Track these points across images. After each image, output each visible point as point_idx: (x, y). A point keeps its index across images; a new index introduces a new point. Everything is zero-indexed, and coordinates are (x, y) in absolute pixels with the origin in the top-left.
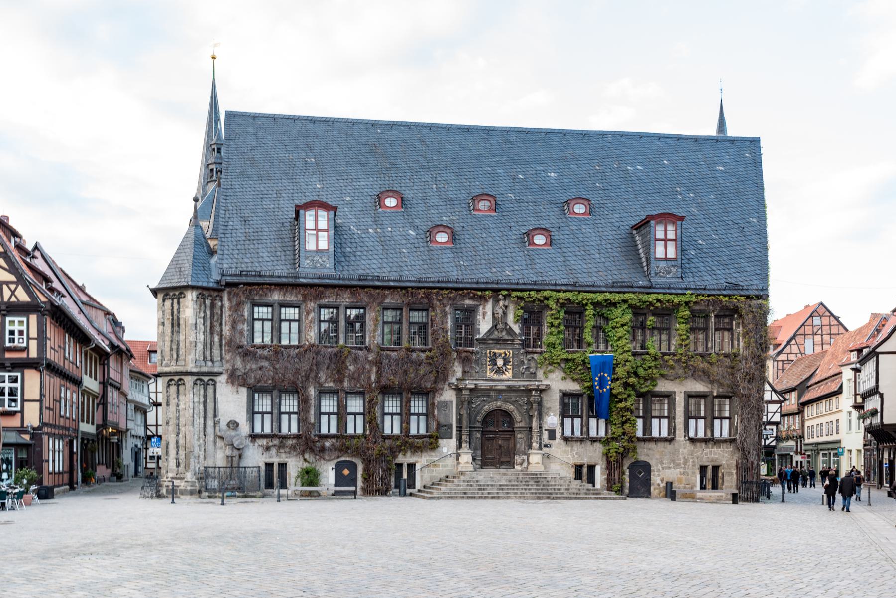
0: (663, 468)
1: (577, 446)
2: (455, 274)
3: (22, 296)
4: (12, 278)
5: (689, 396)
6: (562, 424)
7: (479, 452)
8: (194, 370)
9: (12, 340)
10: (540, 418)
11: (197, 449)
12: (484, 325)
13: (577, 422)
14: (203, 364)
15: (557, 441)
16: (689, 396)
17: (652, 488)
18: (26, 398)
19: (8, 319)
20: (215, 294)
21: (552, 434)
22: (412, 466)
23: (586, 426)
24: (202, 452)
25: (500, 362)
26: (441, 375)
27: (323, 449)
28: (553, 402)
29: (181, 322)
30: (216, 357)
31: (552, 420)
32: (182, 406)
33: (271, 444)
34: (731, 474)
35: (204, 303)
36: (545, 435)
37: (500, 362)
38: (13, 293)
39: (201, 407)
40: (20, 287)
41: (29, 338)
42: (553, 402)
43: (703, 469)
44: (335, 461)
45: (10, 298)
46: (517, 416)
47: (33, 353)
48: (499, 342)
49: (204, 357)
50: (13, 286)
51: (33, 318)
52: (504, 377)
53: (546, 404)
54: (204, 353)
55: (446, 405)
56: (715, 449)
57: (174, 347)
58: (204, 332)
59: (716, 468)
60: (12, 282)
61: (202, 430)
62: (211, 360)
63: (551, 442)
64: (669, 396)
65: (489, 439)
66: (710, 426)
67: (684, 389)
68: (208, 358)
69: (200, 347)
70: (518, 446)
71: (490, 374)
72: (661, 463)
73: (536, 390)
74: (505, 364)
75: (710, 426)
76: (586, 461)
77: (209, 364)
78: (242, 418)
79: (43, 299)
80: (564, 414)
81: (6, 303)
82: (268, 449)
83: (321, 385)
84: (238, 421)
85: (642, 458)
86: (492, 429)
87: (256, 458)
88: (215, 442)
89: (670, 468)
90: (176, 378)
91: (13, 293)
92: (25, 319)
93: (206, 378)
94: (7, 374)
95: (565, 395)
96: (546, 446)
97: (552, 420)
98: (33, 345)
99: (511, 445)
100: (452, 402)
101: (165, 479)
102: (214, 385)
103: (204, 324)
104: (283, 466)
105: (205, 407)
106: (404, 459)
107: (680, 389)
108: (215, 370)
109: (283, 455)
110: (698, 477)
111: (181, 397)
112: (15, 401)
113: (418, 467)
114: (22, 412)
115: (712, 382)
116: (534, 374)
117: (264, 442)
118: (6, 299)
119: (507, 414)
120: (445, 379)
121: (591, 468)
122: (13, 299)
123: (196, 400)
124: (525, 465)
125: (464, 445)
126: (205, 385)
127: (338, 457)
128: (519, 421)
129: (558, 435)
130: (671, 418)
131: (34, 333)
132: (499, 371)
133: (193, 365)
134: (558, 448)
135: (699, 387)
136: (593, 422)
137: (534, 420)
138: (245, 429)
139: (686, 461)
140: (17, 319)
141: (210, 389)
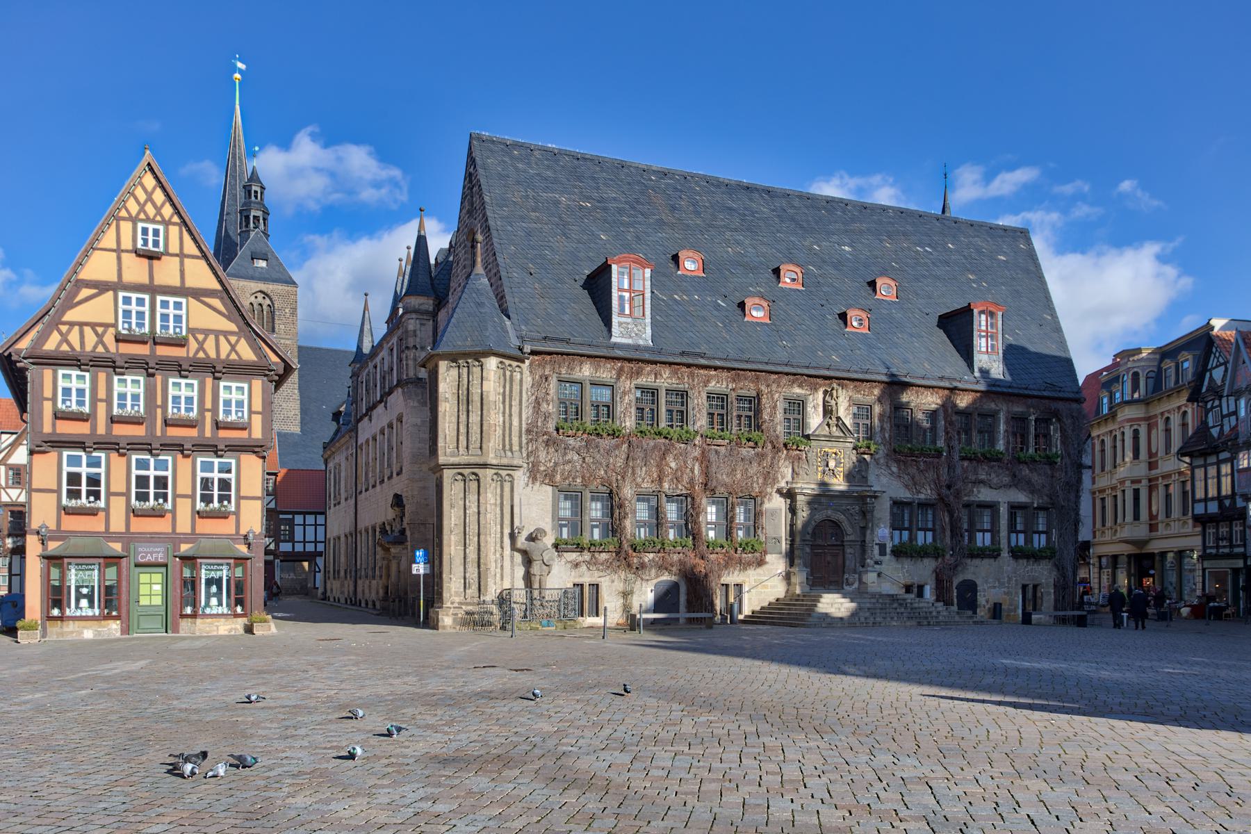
1: (907, 564)
2: (782, 356)
3: (246, 353)
4: (232, 327)
5: (1014, 508)
8: (494, 462)
9: (227, 412)
10: (872, 531)
11: (493, 565)
12: (815, 420)
13: (906, 534)
15: (888, 557)
16: (1014, 508)
18: (242, 494)
19: (222, 384)
20: (515, 364)
21: (882, 547)
22: (739, 586)
23: (912, 538)
24: (499, 570)
26: (769, 476)
27: (642, 566)
28: (883, 510)
29: (476, 398)
30: (516, 448)
31: (883, 532)
32: (472, 509)
33: (580, 559)
34: (1049, 593)
35: (504, 375)
36: (876, 550)
37: (832, 464)
38: (233, 347)
39: (498, 509)
40: (243, 341)
41: (251, 412)
42: (883, 510)
43: (1024, 587)
44: (655, 581)
45: (228, 355)
46: (846, 525)
47: (257, 433)
48: (830, 438)
49: (504, 446)
50: (233, 339)
51: (258, 384)
53: (877, 514)
54: (504, 440)
55: (774, 513)
56: (1035, 567)
57: (463, 429)
58: (504, 413)
59: (1035, 587)
60: (232, 333)
61: (498, 540)
62: (511, 450)
64: (992, 507)
65: (817, 555)
66: (1028, 540)
67: (1007, 500)
68: (507, 447)
69: (499, 431)
70: (847, 563)
72: (987, 582)
73: (871, 497)
75: (1028, 540)
76: (916, 580)
77: (509, 454)
78: (546, 524)
79: (275, 359)
80: (896, 526)
81: (223, 361)
82: (577, 565)
83: (638, 485)
85: (969, 576)
86: (820, 542)
87: (560, 575)
88: (512, 557)
91: (233, 347)
92: (246, 386)
93: (503, 473)
94: (216, 461)
95: (897, 504)
97: (883, 532)
98: (257, 421)
99: (840, 561)
101: (449, 605)
102: (512, 483)
103: (504, 402)
104: (596, 587)
105: (502, 510)
106: (731, 578)
107: (1004, 498)
108: (515, 462)
109: (596, 574)
111: (472, 498)
112: (228, 498)
113: (746, 588)
114: (237, 513)
115: (1032, 492)
116: (865, 478)
117: (573, 556)
118: (223, 356)
119: (836, 525)
120: (775, 480)
121: (921, 588)
122: (233, 356)
123: (492, 501)
124: (856, 585)
125: (796, 561)
126: (502, 481)
127: (657, 576)
128: (851, 535)
129: (888, 550)
130: (994, 531)
131: (258, 405)
134: (890, 565)
135: (1022, 498)
136: (920, 534)
137: (868, 532)
138: (549, 540)
139: (1010, 579)
140: (234, 385)
141: (507, 486)
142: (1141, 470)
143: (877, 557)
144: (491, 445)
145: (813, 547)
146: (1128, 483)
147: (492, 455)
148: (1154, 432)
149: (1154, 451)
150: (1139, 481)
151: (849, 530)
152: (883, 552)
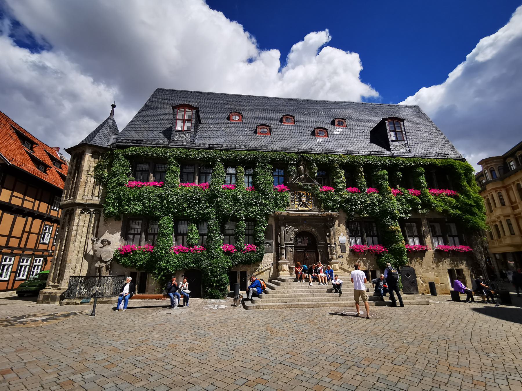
0: (424, 272)
6: (349, 241)
7: (293, 262)
8: (81, 202)
14: (90, 198)
17: (418, 287)
25: (304, 199)
36: (339, 249)
37: (304, 199)
39: (85, 230)
52: (306, 209)
63: (344, 254)
71: (296, 207)
74: (306, 201)
84: (110, 240)
86: (300, 244)
89: (428, 272)
90: (70, 208)
96: (339, 257)
100: (272, 225)
110: (448, 277)
132: (304, 205)
133: (80, 198)
142: (508, 210)
143: (340, 253)
144: (79, 192)
145: (296, 248)
146: (502, 217)
147: (78, 198)
148: (511, 193)
149: (514, 200)
150: (509, 216)
151: (319, 238)
152: (343, 250)
